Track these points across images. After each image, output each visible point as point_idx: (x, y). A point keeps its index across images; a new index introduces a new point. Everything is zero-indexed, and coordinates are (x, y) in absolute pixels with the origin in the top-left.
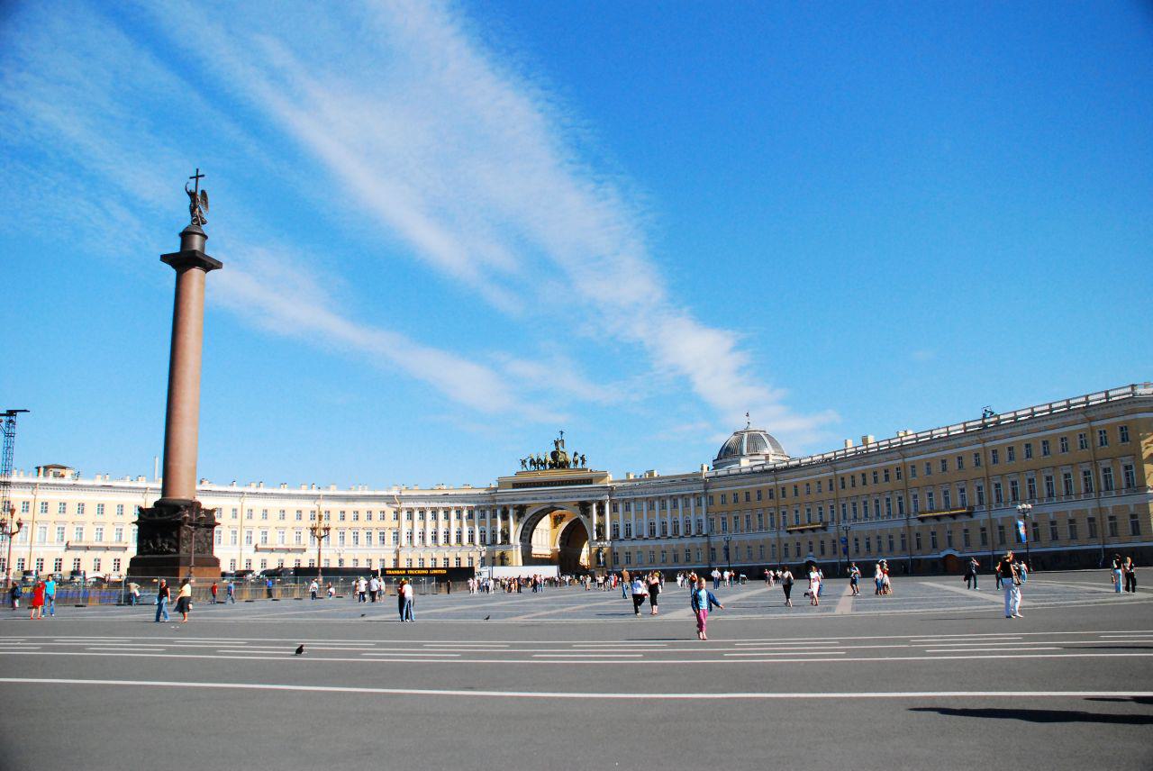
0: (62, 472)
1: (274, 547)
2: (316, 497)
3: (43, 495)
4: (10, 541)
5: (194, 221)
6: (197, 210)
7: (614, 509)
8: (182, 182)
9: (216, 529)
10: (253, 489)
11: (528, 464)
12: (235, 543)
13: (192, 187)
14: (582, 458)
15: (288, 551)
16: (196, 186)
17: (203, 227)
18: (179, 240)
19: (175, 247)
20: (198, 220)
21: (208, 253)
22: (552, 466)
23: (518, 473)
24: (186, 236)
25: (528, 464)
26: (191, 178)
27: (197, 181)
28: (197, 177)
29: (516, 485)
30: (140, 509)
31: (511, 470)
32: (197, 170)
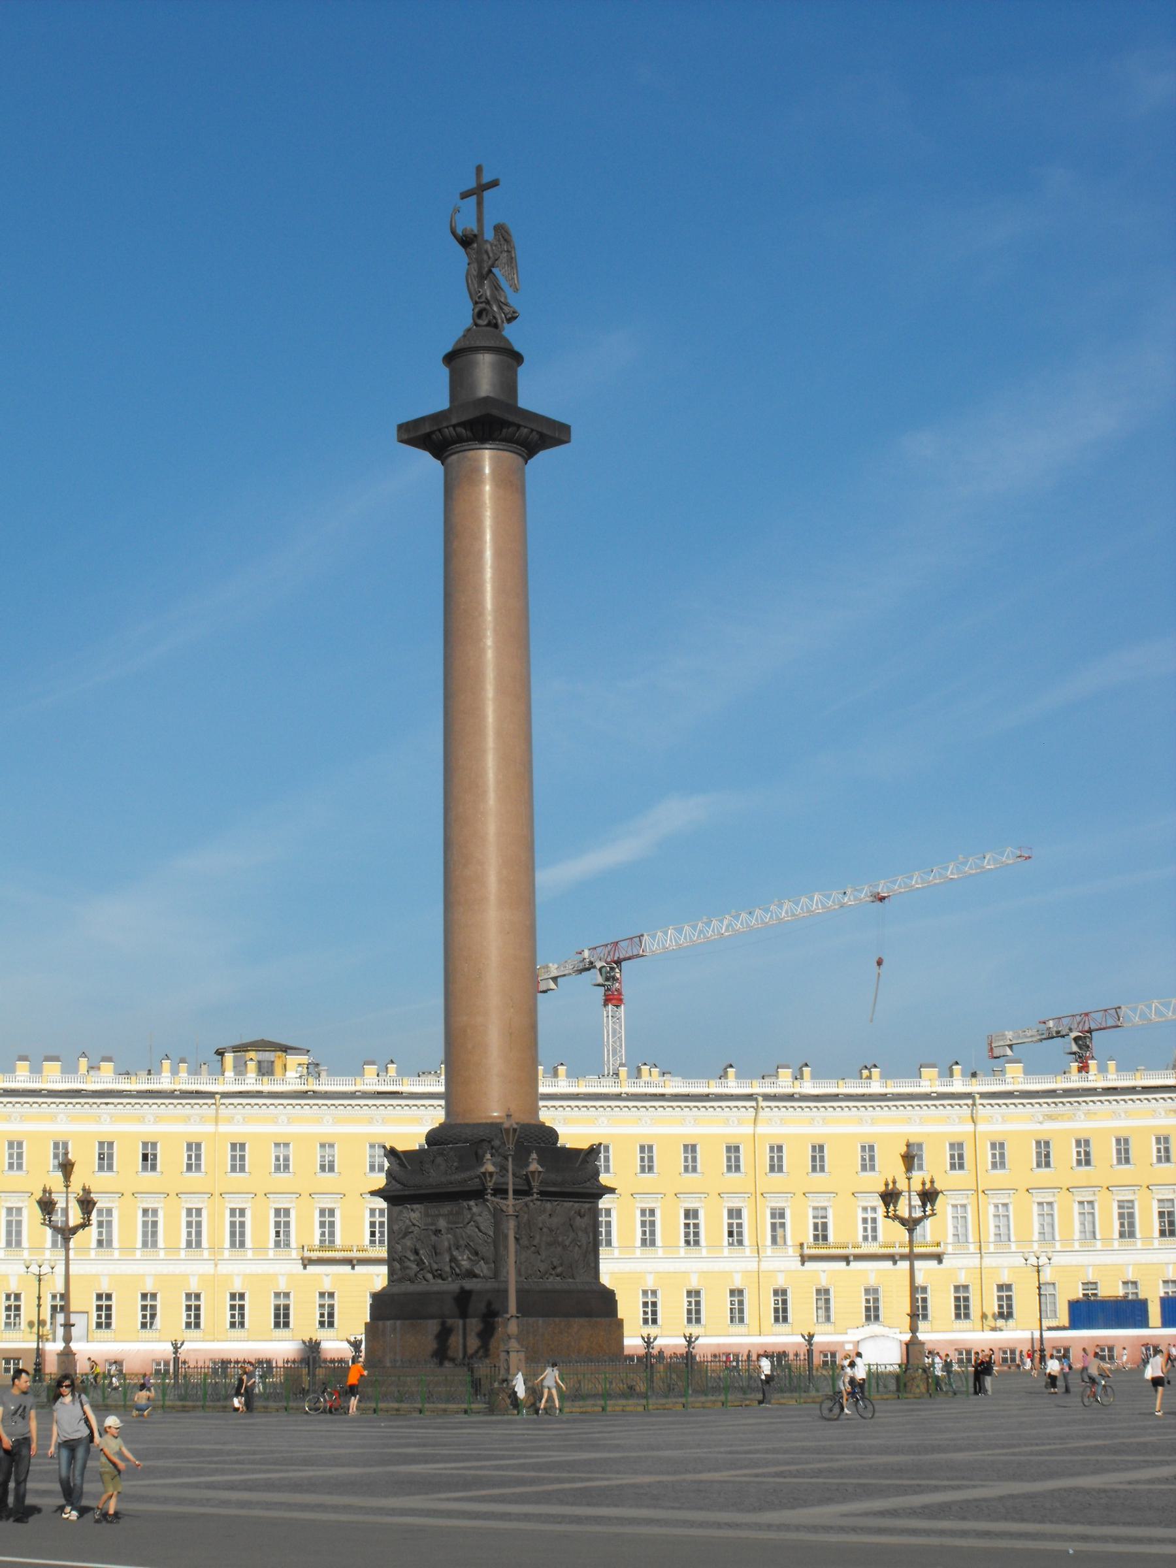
5: (479, 315)
9: (604, 1203)
10: (784, 1083)
13: (467, 222)
16: (480, 220)
18: (444, 373)
19: (433, 397)
26: (465, 195)
27: (480, 204)
28: (480, 189)
30: (392, 1153)
32: (479, 169)
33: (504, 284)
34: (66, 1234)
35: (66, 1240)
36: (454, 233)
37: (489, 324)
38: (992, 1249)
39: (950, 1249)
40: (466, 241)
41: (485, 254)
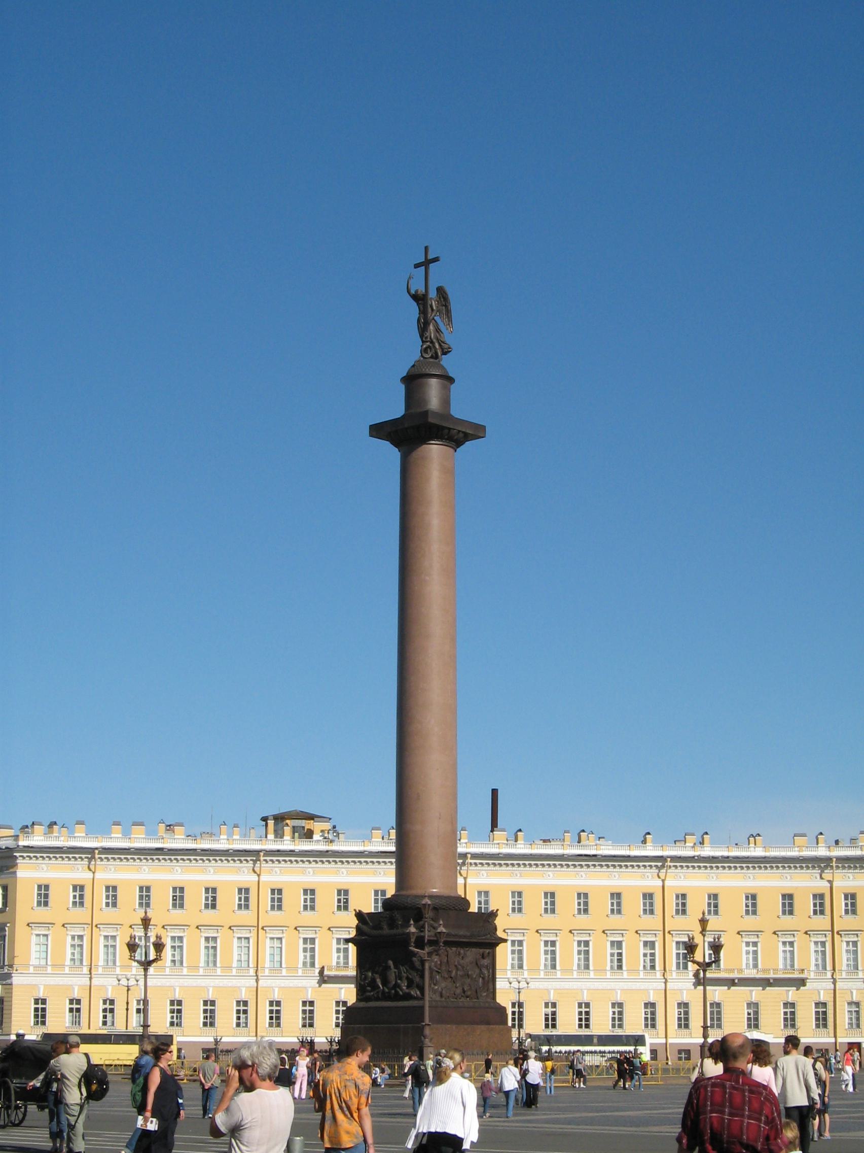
0: (308, 824)
1: (735, 975)
2: (822, 864)
3: (275, 875)
4: (146, 976)
5: (425, 350)
6: (431, 327)
12: (653, 967)
13: (418, 286)
15: (766, 983)
17: (446, 361)
18: (402, 388)
19: (394, 407)
21: (457, 411)
24: (413, 381)
26: (417, 266)
28: (426, 263)
32: (426, 248)
33: (442, 327)
34: (146, 964)
35: (146, 970)
36: (409, 291)
37: (432, 357)
38: (844, 975)
39: (812, 975)
40: (416, 297)
41: (430, 307)
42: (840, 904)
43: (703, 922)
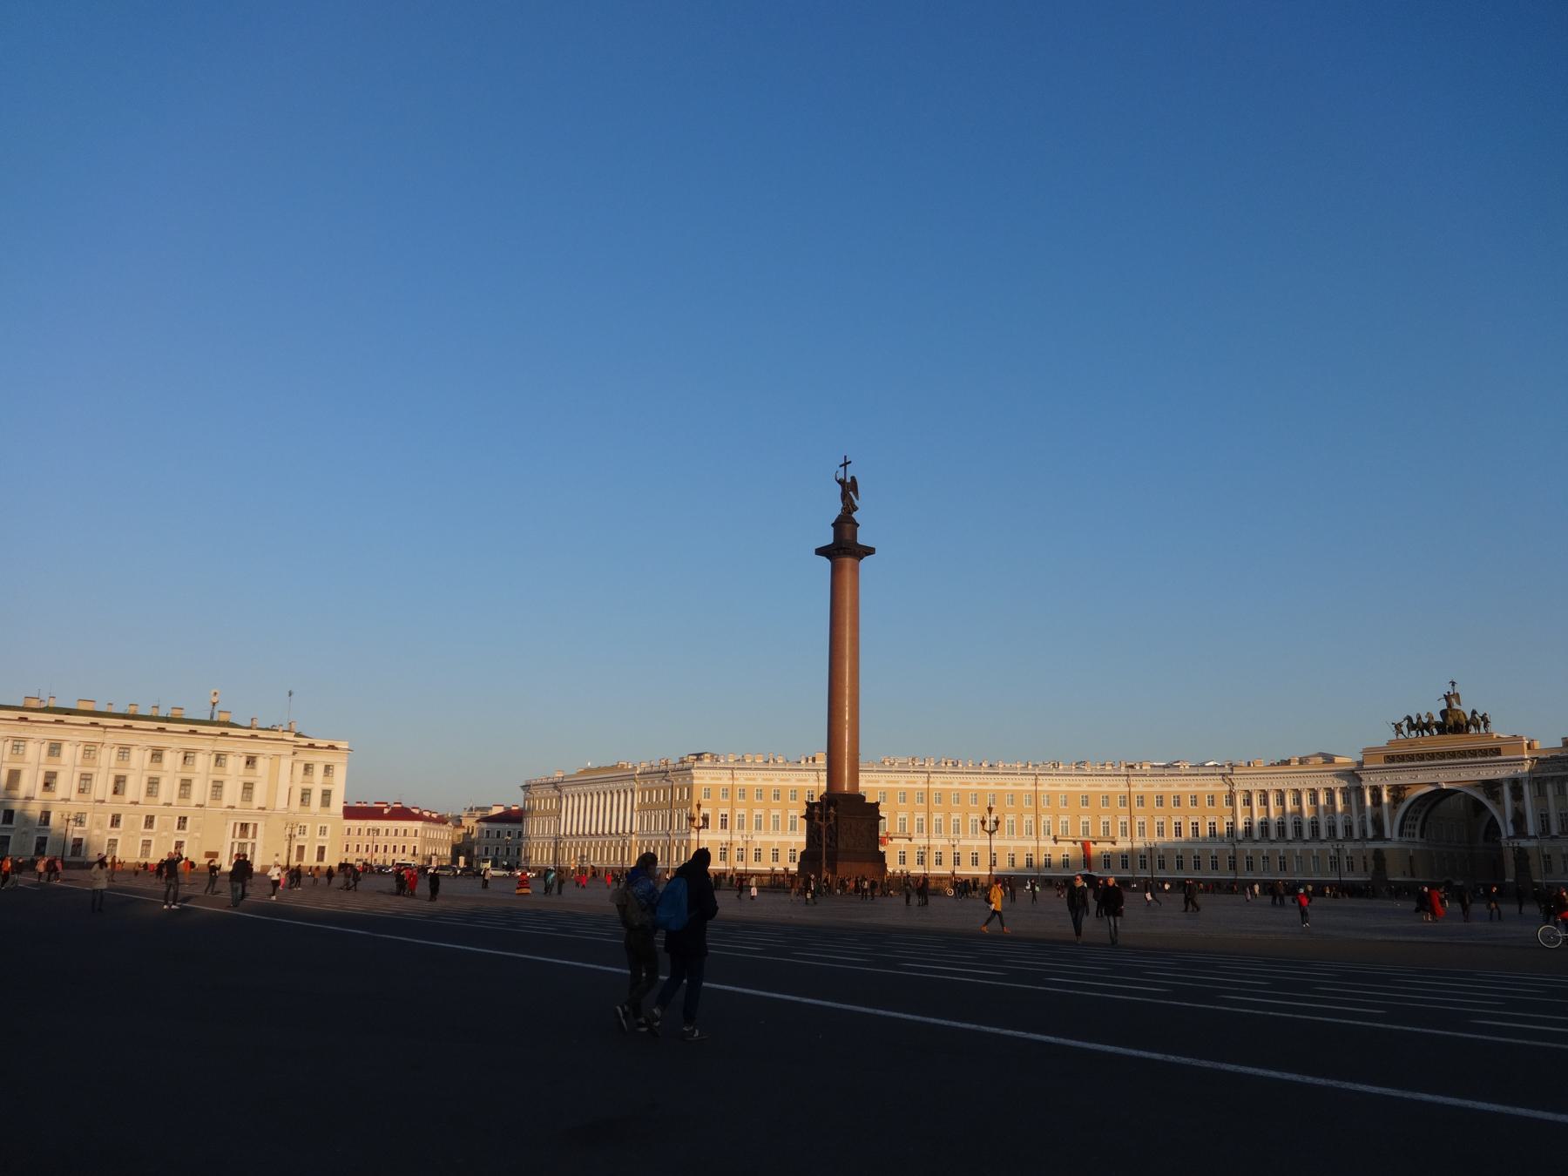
7: (1541, 793)
8: (833, 470)
11: (1405, 729)
13: (841, 476)
14: (1483, 718)
17: (855, 515)
18: (832, 529)
19: (828, 539)
20: (849, 508)
22: (1442, 728)
23: (1390, 743)
24: (838, 525)
25: (1405, 729)
28: (845, 464)
29: (1390, 759)
31: (1383, 736)
42: (1135, 801)
43: (990, 809)
